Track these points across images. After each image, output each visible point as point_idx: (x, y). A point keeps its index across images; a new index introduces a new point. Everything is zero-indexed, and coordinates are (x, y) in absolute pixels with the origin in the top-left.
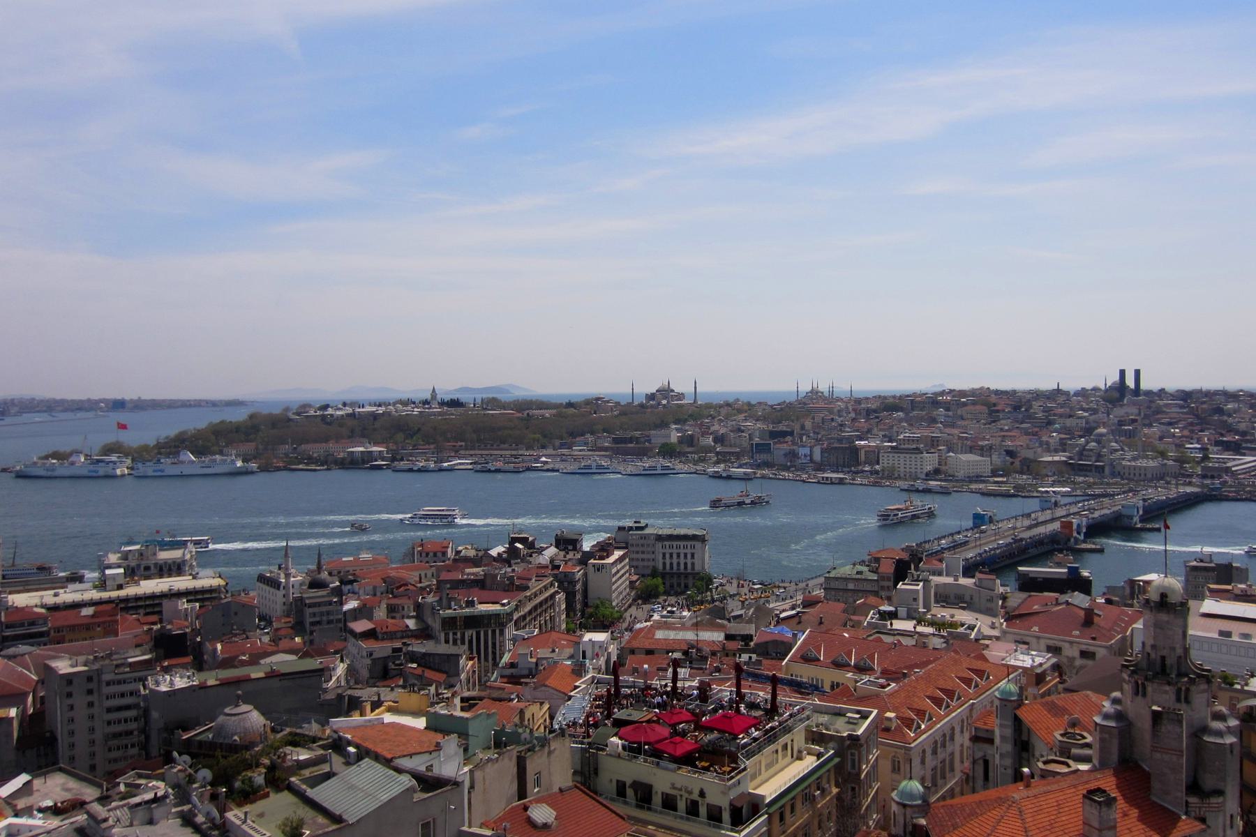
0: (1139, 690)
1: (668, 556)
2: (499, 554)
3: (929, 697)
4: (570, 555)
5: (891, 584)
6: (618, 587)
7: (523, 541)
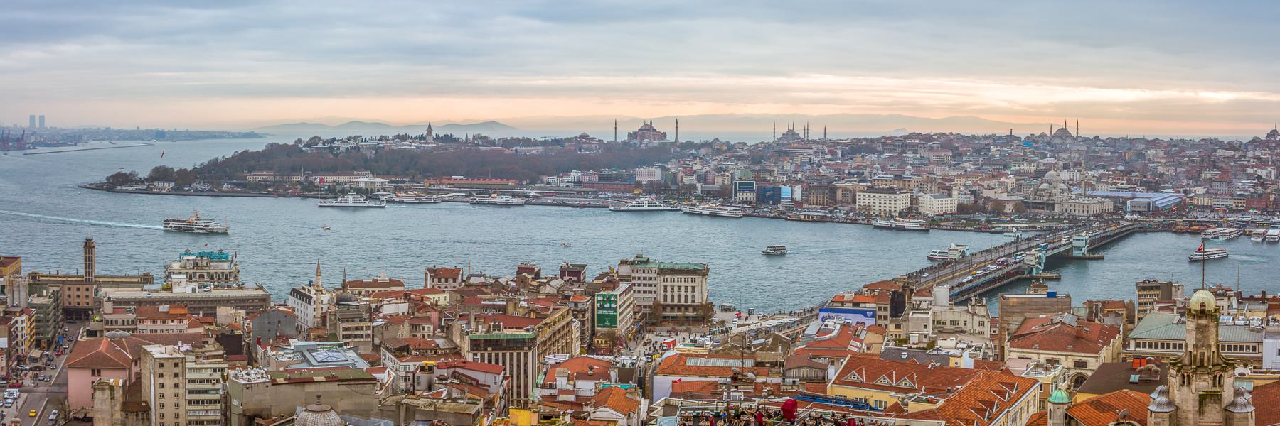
0: (1186, 381)
1: (669, 289)
3: (972, 408)
7: (530, 270)
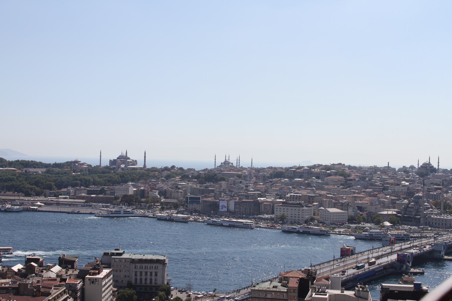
2: (19, 269)
4: (70, 272)
5: (296, 294)
6: (106, 295)
